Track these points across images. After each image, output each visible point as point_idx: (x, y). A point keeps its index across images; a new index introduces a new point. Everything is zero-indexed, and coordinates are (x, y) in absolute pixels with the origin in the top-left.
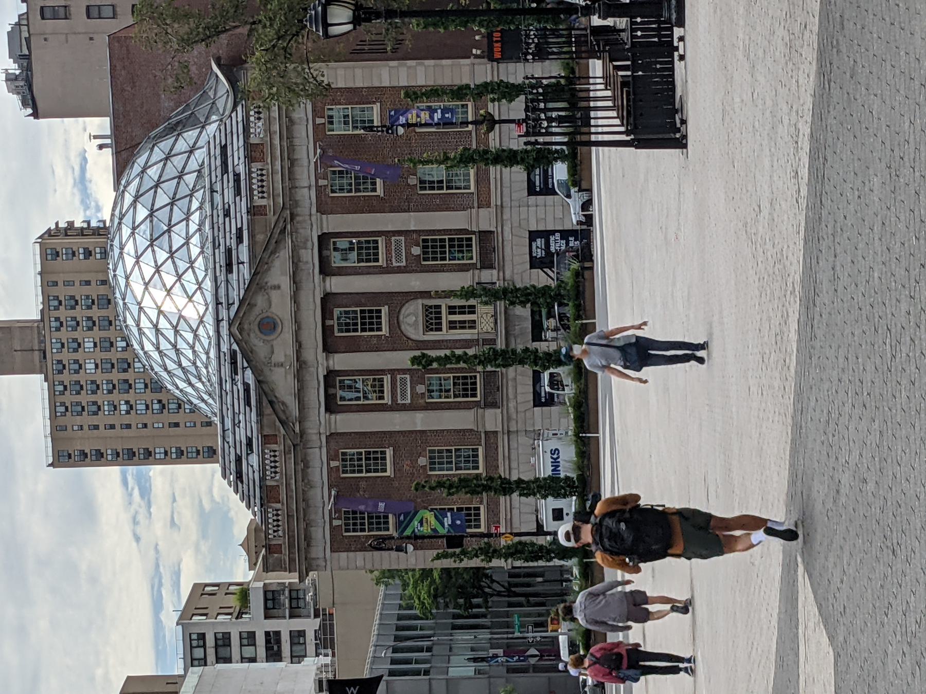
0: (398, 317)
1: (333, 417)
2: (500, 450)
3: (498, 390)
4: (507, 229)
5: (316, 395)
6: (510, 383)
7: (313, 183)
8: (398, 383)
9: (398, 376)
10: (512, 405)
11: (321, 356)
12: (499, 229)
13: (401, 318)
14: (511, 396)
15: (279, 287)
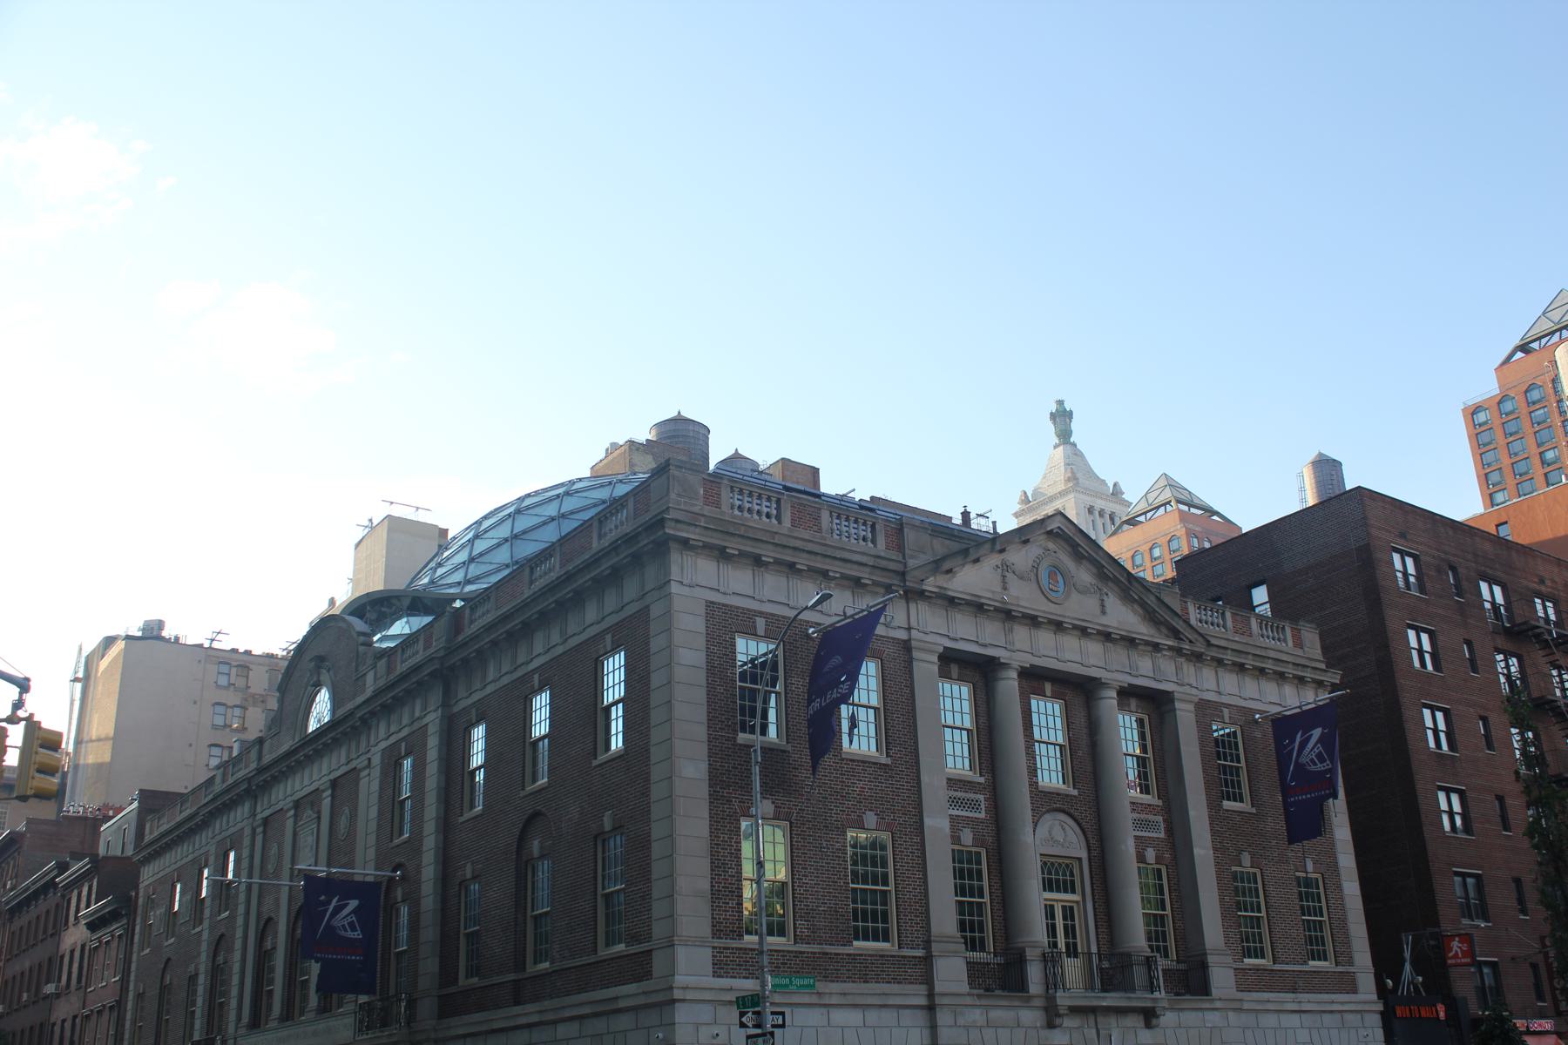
0: (1063, 811)
1: (935, 659)
2: (895, 988)
3: (987, 990)
4: (1213, 1018)
5: (970, 634)
6: (1010, 1014)
7: (1225, 700)
8: (972, 796)
9: (981, 797)
10: (976, 1016)
11: (1028, 660)
12: (1218, 1004)
13: (1062, 817)
14: (996, 1014)
15: (1104, 612)
